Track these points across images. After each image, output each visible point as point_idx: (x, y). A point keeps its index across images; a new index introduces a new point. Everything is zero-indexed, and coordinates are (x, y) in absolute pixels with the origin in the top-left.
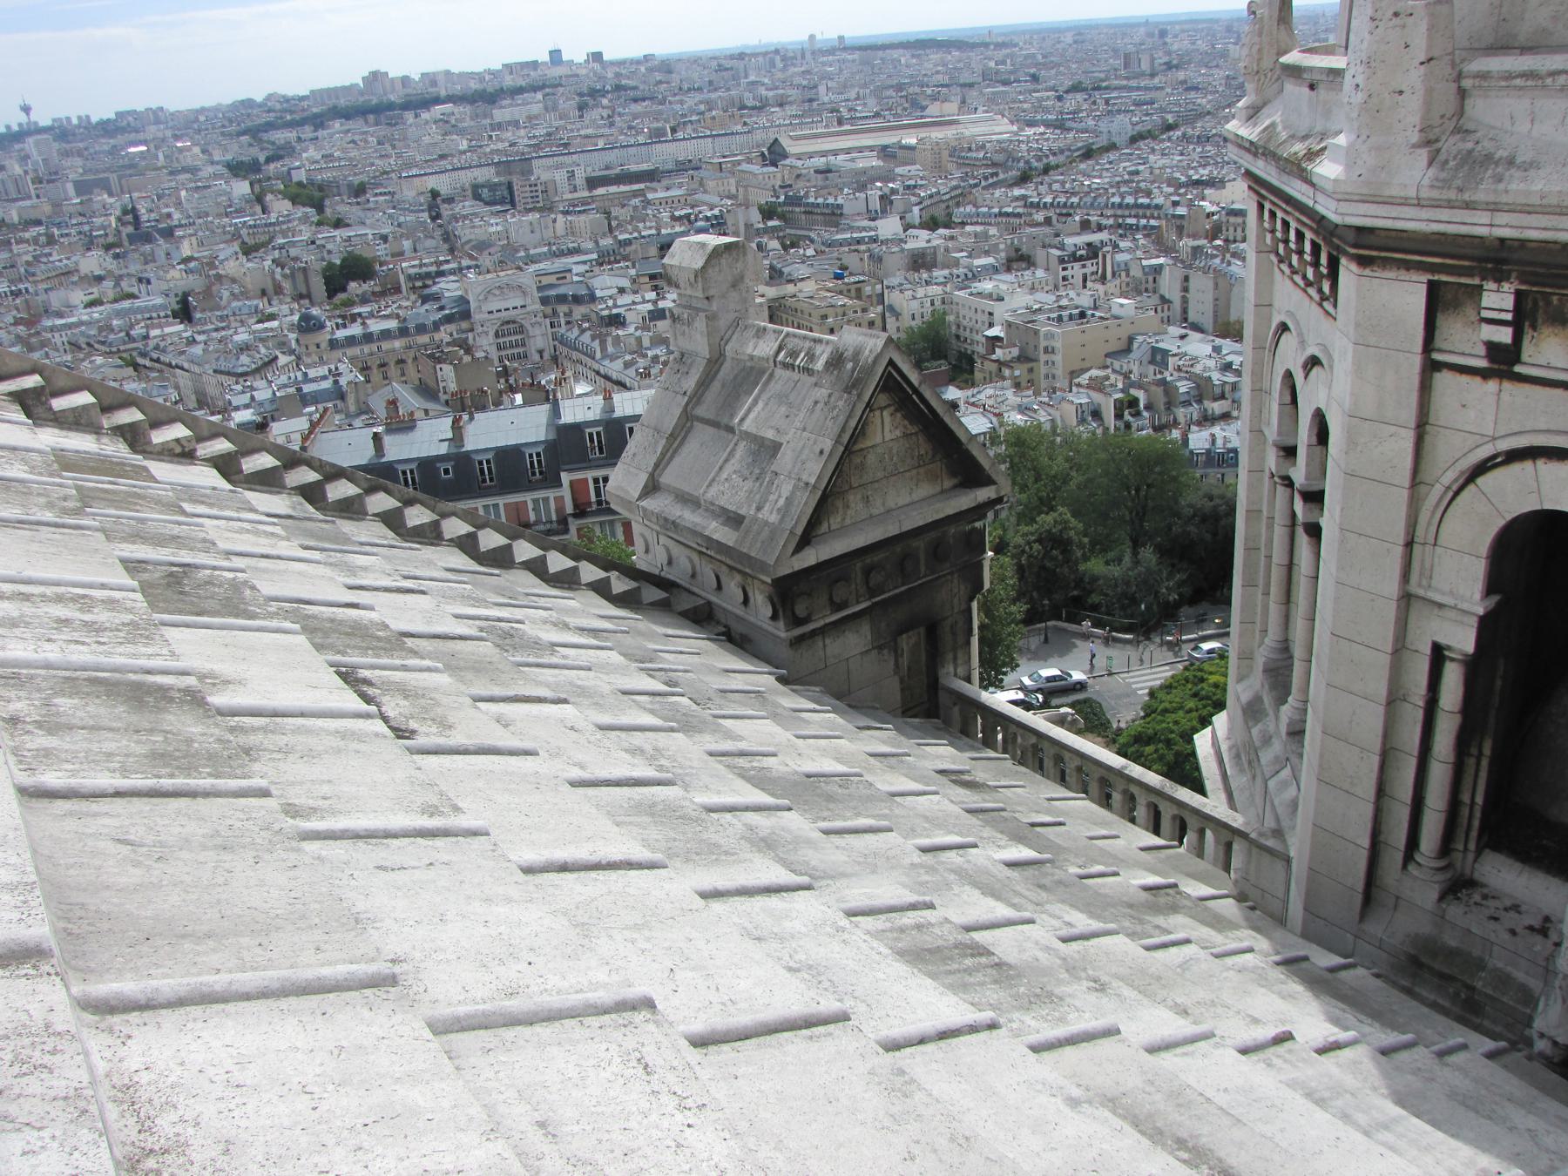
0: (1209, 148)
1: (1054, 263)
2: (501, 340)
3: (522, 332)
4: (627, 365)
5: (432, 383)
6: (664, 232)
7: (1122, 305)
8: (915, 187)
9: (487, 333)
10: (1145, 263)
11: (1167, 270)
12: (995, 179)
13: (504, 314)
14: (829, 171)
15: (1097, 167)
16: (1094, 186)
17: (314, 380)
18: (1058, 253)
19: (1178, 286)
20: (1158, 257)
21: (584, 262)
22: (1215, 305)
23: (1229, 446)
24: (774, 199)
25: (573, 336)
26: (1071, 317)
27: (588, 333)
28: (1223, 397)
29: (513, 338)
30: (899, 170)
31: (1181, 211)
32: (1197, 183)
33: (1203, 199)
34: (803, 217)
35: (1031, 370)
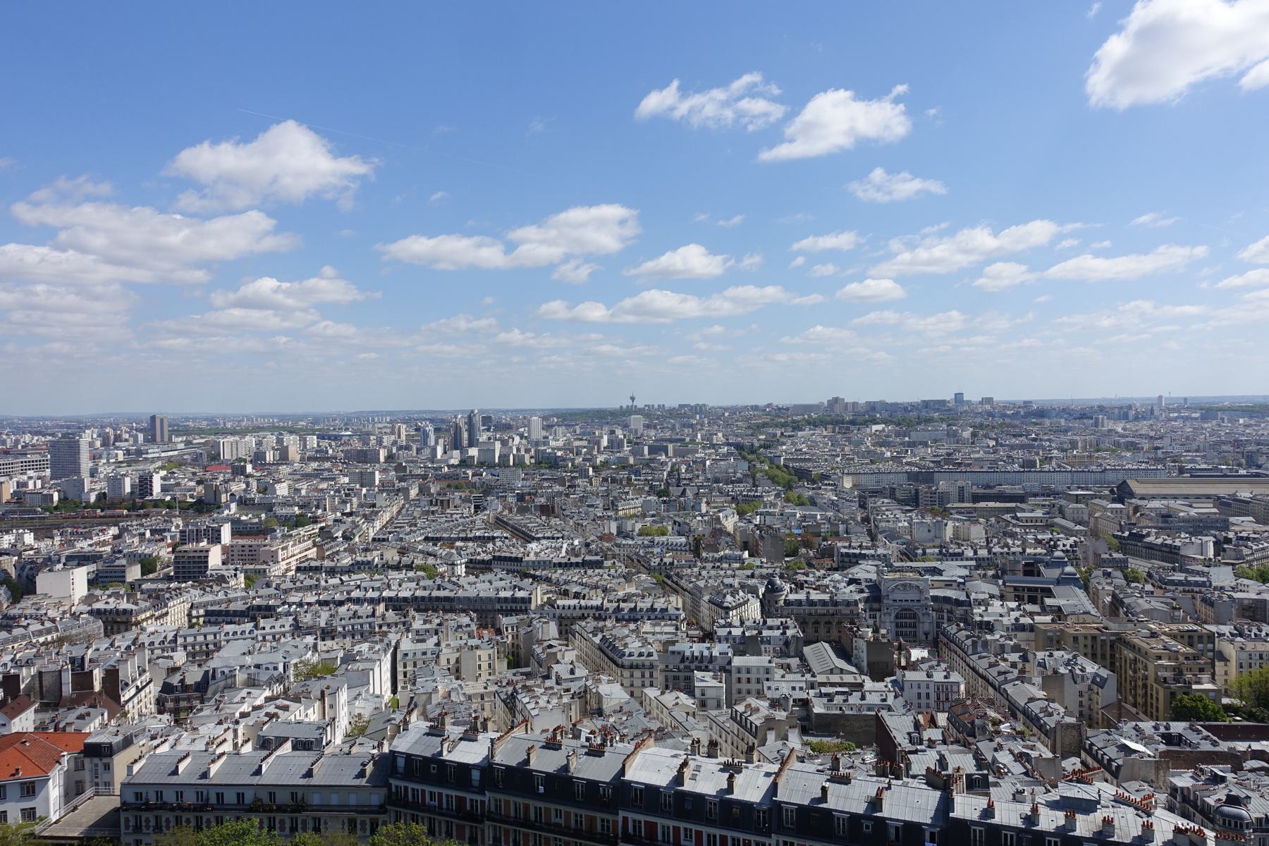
2: (900, 621)
3: (915, 618)
4: (991, 666)
5: (848, 649)
6: (1028, 551)
8: (1248, 539)
9: (890, 614)
13: (904, 603)
14: (1170, 516)
17: (771, 628)
21: (965, 567)
24: (1120, 533)
25: (953, 632)
27: (964, 633)
29: (908, 621)
30: (1232, 519)
34: (1144, 550)
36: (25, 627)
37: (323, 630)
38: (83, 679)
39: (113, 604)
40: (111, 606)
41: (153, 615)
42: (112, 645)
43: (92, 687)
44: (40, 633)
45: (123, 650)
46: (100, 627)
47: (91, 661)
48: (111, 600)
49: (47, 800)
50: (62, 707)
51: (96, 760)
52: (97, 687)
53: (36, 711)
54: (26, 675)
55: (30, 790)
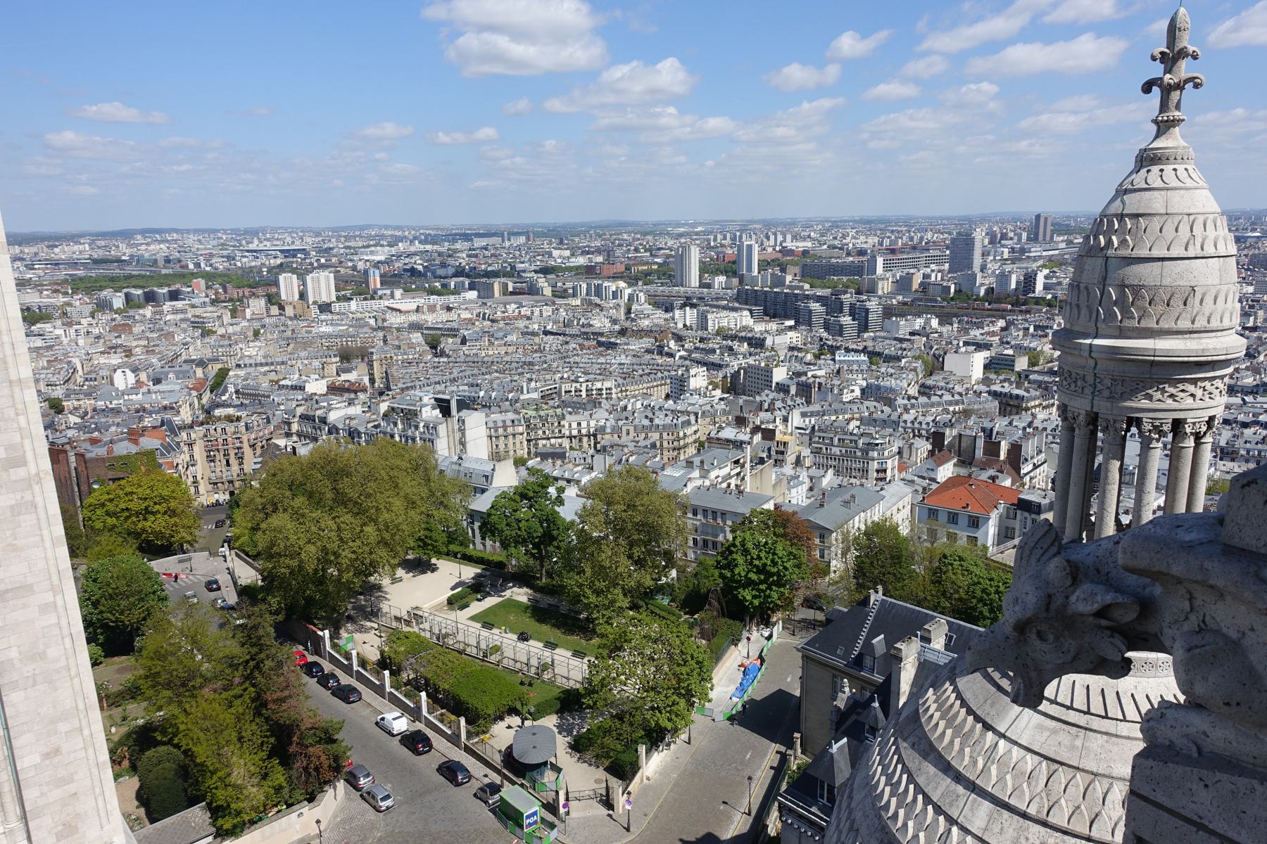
36: (941, 396)
37: (1222, 449)
38: (992, 448)
39: (1007, 388)
40: (1006, 390)
41: (1041, 404)
42: (1011, 423)
43: (999, 456)
44: (950, 403)
45: (1049, 431)
46: (995, 407)
47: (997, 433)
48: (1006, 385)
49: (987, 534)
50: (976, 466)
51: (1026, 514)
52: (1003, 456)
53: (955, 465)
54: (950, 435)
55: (975, 523)
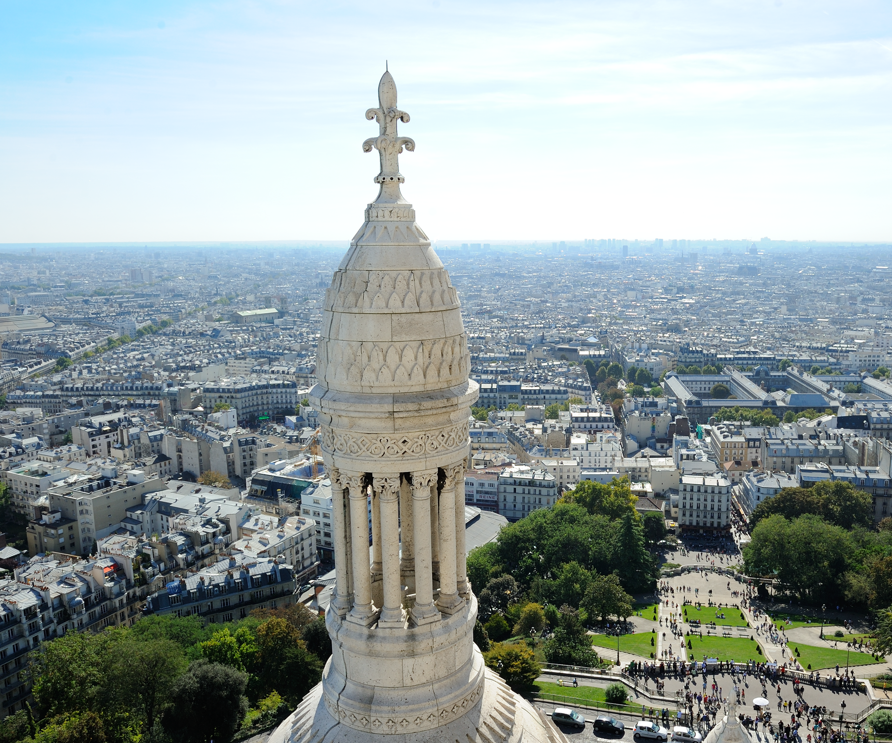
0: (190, 340)
1: (86, 437)
7: (135, 475)
10: (150, 434)
11: (166, 439)
12: (39, 366)
15: (115, 356)
16: (113, 371)
18: (89, 430)
19: (174, 448)
20: (160, 429)
22: (200, 461)
23: (213, 583)
26: (99, 487)
28: (207, 542)
31: (175, 389)
32: (184, 367)
33: (188, 379)
35: (71, 528)
